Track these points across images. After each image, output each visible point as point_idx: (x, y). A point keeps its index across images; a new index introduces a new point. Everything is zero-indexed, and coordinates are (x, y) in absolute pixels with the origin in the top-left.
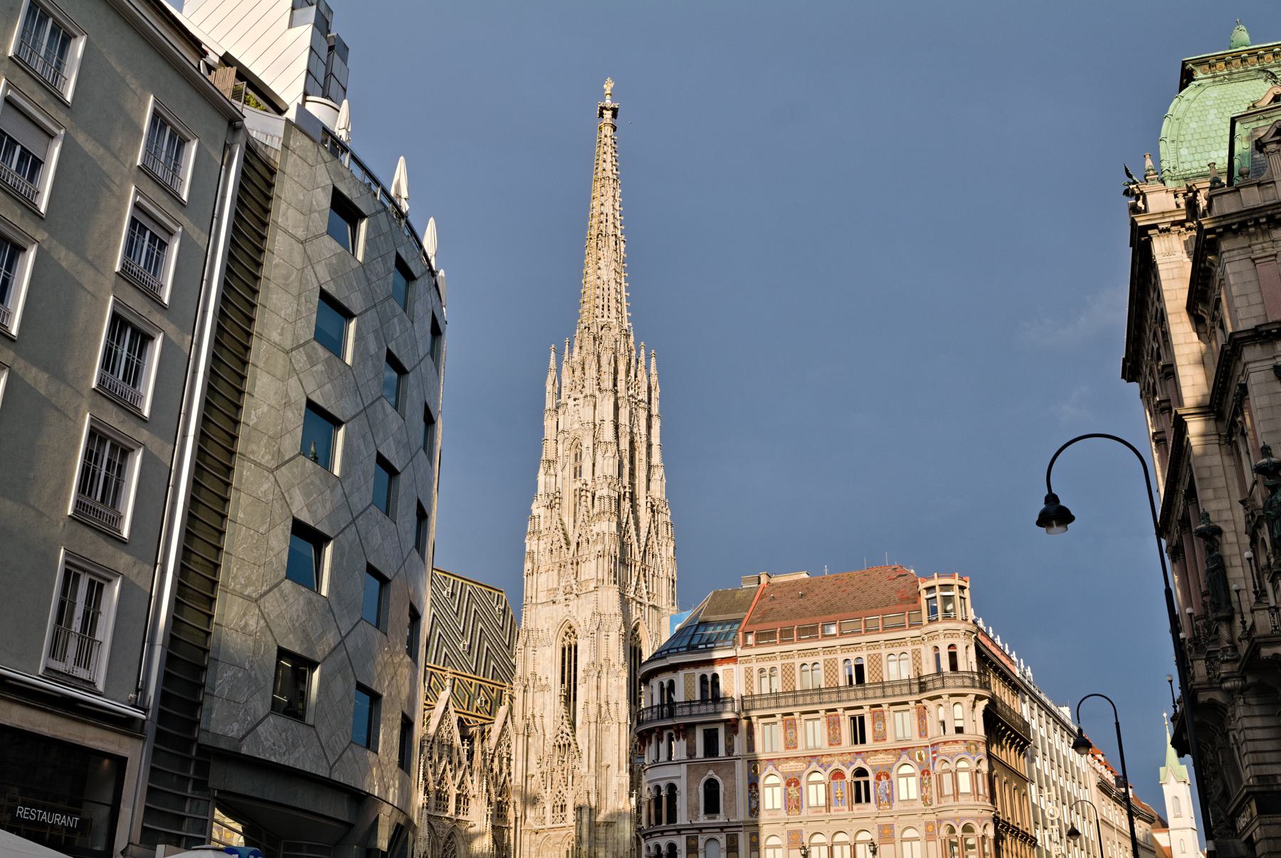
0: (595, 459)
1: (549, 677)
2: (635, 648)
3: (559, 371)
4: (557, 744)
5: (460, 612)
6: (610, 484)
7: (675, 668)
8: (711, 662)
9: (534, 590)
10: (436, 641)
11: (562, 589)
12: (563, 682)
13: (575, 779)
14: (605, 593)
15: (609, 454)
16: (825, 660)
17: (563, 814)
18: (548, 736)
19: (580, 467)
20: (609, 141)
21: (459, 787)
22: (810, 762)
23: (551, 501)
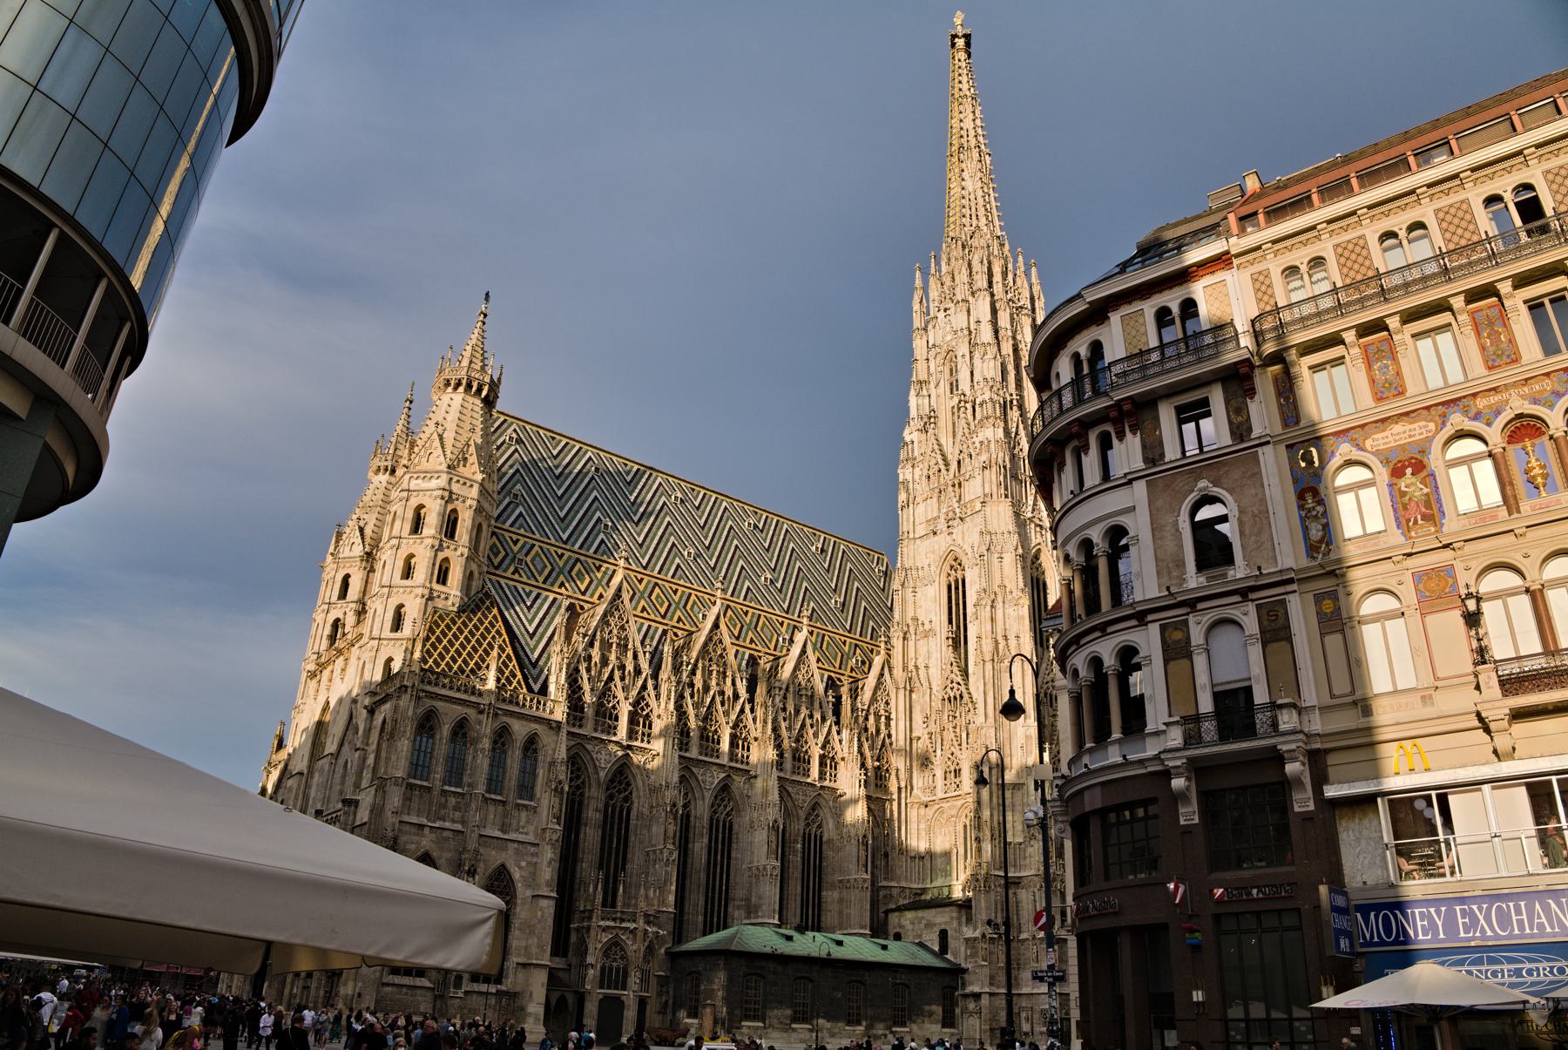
0: (972, 364)
1: (933, 620)
2: (1038, 580)
3: (925, 289)
4: (946, 697)
5: (832, 568)
6: (992, 387)
7: (1098, 313)
8: (1184, 276)
9: (911, 523)
10: (802, 594)
11: (943, 516)
12: (950, 622)
13: (971, 736)
14: (995, 508)
15: (990, 356)
16: (1437, 211)
17: (957, 781)
18: (934, 691)
19: (957, 381)
20: (963, 64)
21: (823, 747)
22: (1444, 415)
23: (926, 423)
